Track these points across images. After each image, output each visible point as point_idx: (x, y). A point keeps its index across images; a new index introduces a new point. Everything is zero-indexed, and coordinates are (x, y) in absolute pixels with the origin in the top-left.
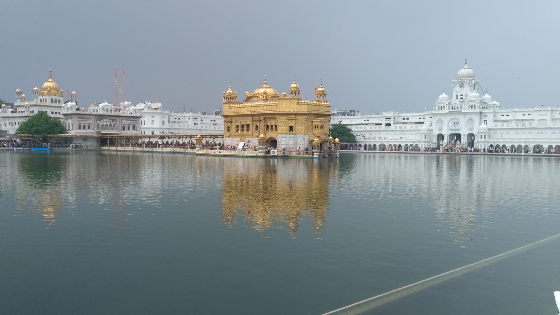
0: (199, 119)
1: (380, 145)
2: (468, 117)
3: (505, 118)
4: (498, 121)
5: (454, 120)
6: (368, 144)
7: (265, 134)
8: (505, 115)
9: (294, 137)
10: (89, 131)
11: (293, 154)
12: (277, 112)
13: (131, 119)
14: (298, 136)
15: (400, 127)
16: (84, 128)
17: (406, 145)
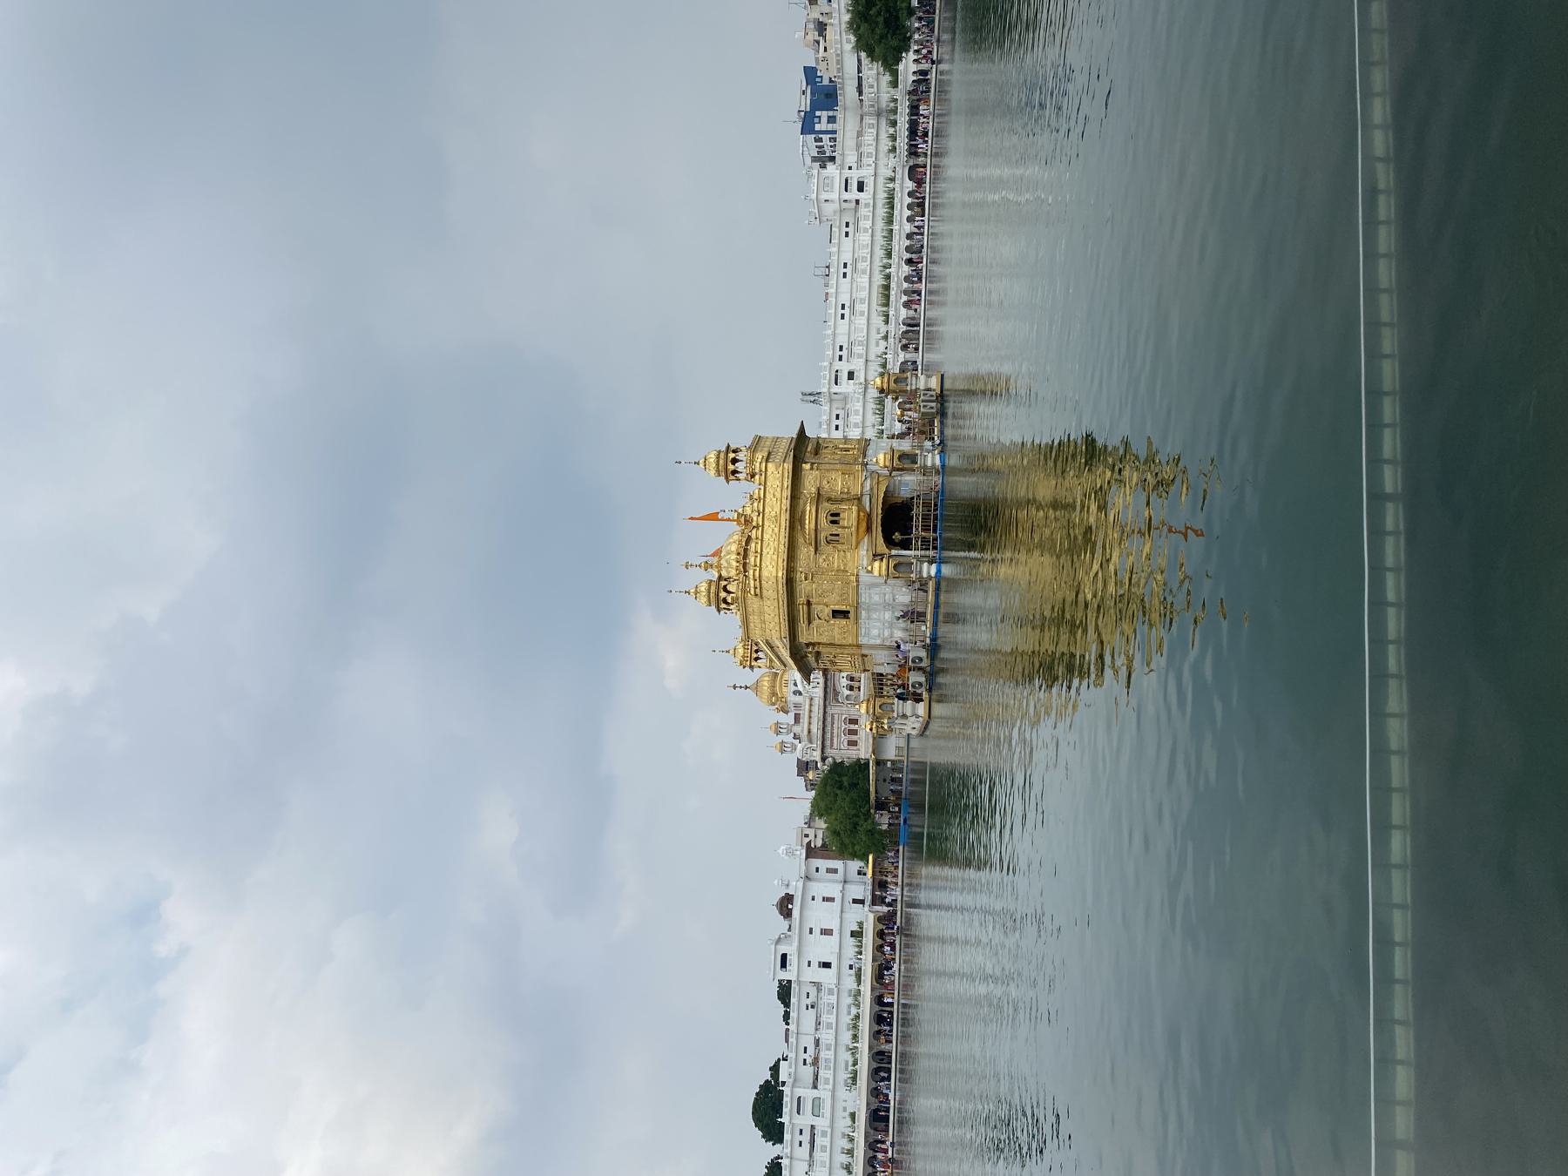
0: (838, 365)
9: (868, 610)
16: (855, 732)
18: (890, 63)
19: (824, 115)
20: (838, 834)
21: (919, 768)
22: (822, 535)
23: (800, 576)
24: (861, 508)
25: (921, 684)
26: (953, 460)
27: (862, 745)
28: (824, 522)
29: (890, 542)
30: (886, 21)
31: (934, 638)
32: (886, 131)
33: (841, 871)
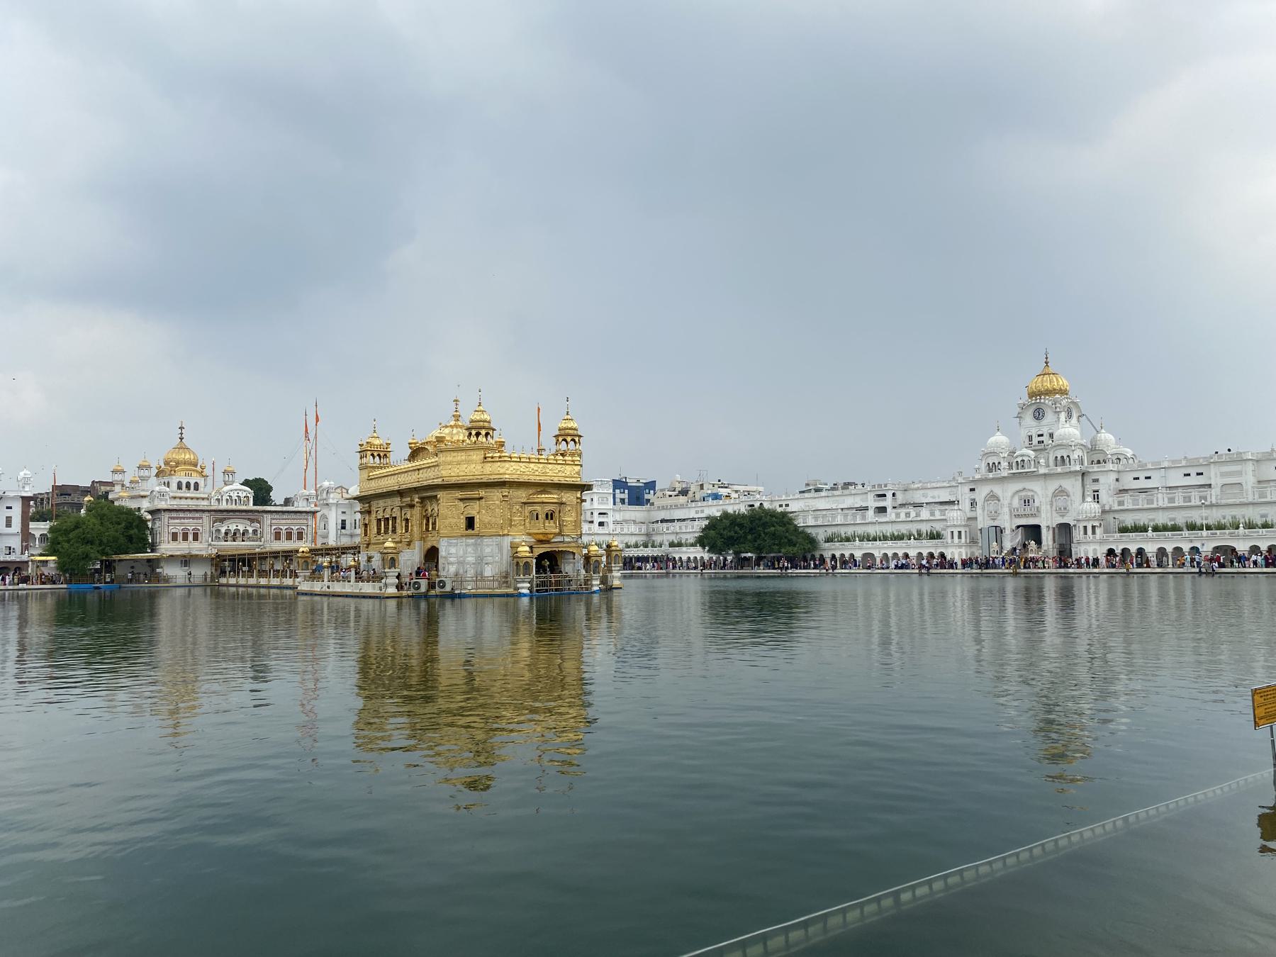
1: (865, 555)
2: (1053, 485)
3: (1142, 484)
4: (1126, 491)
5: (1023, 494)
6: (838, 555)
7: (423, 539)
8: (1142, 478)
9: (475, 545)
10: (196, 545)
11: (469, 588)
12: (439, 481)
13: (293, 516)
14: (486, 540)
15: (908, 515)
16: (185, 537)
17: (920, 554)
18: (701, 542)
19: (625, 496)
20: (77, 527)
21: (153, 596)
22: (538, 508)
23: (505, 491)
24: (556, 535)
25: (418, 588)
26: (596, 598)
27: (173, 545)
28: (548, 508)
29: (540, 558)
30: (731, 538)
31: (461, 596)
32: (641, 539)
33: (9, 530)
